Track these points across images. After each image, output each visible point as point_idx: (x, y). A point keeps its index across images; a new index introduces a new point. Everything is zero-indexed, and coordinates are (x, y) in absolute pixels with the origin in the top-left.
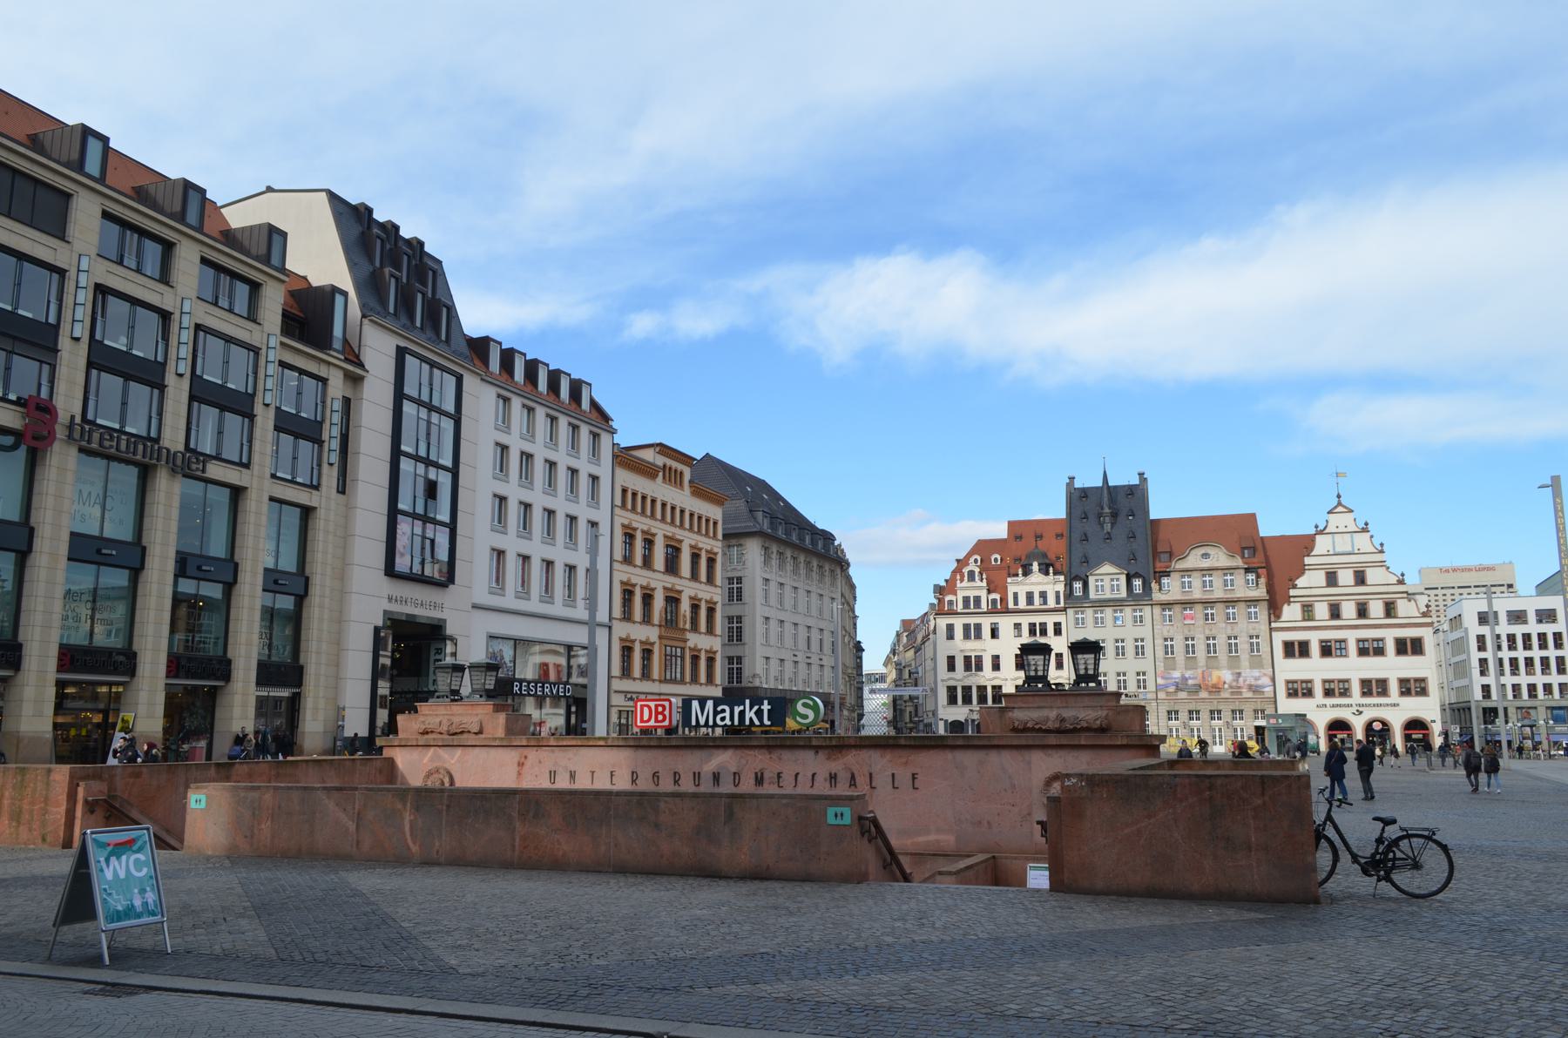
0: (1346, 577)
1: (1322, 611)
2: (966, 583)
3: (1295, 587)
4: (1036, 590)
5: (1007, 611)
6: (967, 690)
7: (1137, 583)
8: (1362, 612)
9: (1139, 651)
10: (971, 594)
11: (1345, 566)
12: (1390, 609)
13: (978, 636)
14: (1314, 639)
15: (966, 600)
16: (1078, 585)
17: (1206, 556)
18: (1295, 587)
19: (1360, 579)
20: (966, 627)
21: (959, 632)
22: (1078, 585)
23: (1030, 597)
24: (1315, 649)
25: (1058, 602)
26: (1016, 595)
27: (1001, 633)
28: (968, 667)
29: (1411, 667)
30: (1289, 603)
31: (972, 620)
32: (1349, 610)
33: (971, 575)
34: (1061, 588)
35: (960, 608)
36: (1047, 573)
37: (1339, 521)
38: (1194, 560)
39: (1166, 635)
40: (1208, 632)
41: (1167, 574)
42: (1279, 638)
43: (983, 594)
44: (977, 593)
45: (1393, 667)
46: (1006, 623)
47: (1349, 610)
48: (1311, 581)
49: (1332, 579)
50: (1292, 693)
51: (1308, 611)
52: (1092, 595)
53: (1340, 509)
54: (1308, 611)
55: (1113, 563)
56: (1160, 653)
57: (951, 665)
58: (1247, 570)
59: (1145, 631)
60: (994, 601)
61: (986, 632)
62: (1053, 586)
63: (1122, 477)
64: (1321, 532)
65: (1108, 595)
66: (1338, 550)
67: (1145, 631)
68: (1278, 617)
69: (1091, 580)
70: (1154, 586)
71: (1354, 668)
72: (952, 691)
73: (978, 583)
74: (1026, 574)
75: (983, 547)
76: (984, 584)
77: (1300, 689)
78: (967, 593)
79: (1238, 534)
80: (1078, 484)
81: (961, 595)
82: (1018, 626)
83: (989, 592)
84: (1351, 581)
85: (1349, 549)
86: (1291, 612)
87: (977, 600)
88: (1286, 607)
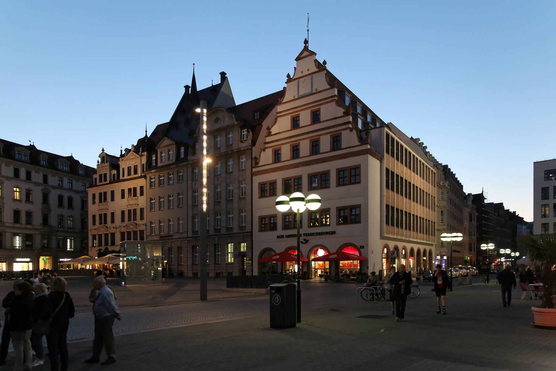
0: (305, 118)
8: (315, 146)
31: (102, 189)
34: (144, 160)
42: (258, 179)
48: (281, 126)
49: (295, 123)
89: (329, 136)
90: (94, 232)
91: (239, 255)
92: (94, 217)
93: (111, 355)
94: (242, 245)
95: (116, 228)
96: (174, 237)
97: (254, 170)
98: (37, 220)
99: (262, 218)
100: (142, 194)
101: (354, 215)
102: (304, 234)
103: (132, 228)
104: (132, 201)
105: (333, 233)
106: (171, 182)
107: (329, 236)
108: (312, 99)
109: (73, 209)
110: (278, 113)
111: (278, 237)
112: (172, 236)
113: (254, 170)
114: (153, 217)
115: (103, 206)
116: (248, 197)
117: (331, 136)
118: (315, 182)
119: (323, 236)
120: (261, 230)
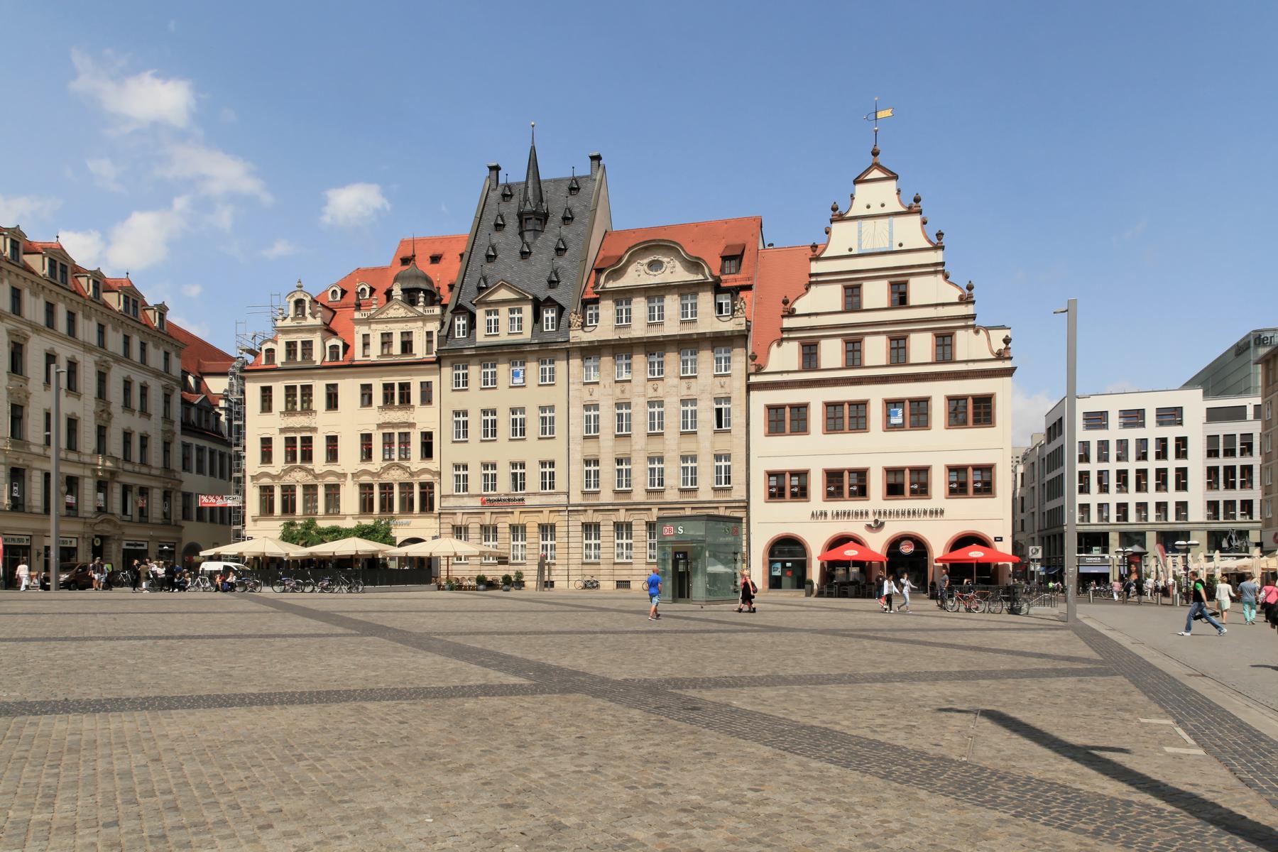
0: (876, 294)
1: (831, 353)
3: (791, 314)
4: (397, 330)
9: (547, 427)
10: (299, 338)
13: (308, 410)
15: (291, 346)
17: (655, 265)
22: (461, 322)
23: (386, 339)
24: (816, 417)
25: (429, 351)
26: (366, 336)
28: (290, 455)
29: (971, 446)
30: (780, 342)
32: (876, 350)
34: (434, 327)
35: (280, 358)
38: (636, 275)
39: (588, 399)
40: (651, 393)
43: (317, 339)
44: (306, 337)
45: (941, 446)
46: (349, 388)
47: (876, 350)
50: (776, 494)
52: (481, 336)
54: (810, 353)
55: (510, 287)
56: (578, 429)
57: (267, 456)
59: (554, 396)
64: (839, 217)
65: (504, 337)
67: (554, 396)
69: (480, 314)
71: (876, 450)
72: (267, 491)
76: (318, 321)
77: (789, 486)
78: (291, 338)
81: (282, 340)
82: (366, 390)
87: (307, 345)
92: (266, 443)
98: (87, 439)
103: (395, 476)
105: (939, 513)
106: (519, 381)
109: (149, 416)
110: (811, 275)
113: (753, 379)
115: (298, 421)
118: (896, 414)
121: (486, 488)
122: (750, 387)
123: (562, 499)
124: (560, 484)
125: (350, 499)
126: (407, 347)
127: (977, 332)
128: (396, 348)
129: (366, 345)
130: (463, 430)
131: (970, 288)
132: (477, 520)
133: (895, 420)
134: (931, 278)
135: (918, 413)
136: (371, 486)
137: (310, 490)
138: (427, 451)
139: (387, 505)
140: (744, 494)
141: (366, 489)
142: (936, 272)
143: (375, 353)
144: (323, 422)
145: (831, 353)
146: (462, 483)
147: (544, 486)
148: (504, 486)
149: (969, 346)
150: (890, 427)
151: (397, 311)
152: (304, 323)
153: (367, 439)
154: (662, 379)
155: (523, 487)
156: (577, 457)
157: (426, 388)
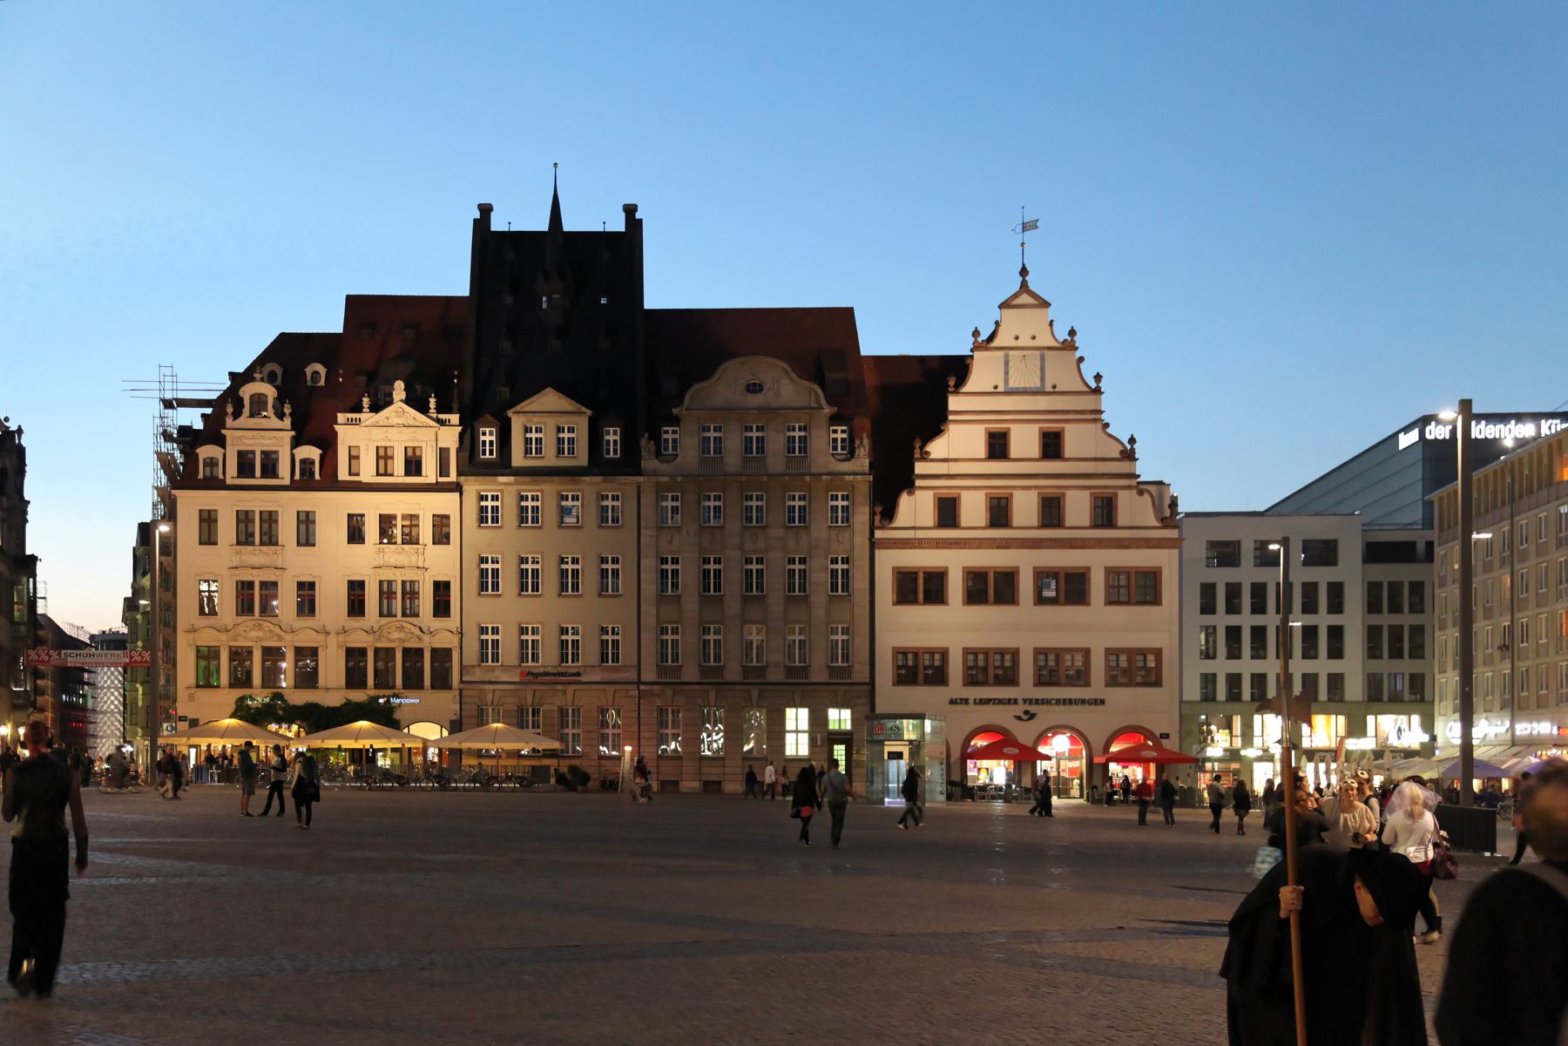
0: (1024, 441)
1: (973, 509)
2: (244, 420)
3: (925, 457)
5: (331, 482)
6: (240, 656)
7: (612, 436)
8: (1052, 511)
11: (1026, 416)
12: (1105, 511)
14: (955, 563)
16: (488, 436)
18: (925, 457)
19: (1052, 446)
20: (244, 518)
21: (227, 529)
22: (488, 436)
23: (383, 456)
24: (955, 587)
25: (443, 469)
27: (322, 530)
31: (257, 502)
32: (1025, 508)
33: (258, 403)
34: (450, 437)
36: (424, 409)
37: (1020, 328)
41: (676, 421)
42: (889, 561)
47: (1025, 508)
48: (956, 446)
49: (998, 446)
51: (948, 511)
52: (518, 459)
53: (1025, 299)
56: (650, 587)
58: (835, 420)
60: (307, 464)
61: (287, 530)
62: (434, 436)
63: (590, 215)
64: (986, 344)
66: (1013, 384)
68: (889, 513)
70: (645, 443)
72: (207, 656)
73: (275, 422)
74: (375, 408)
75: (288, 352)
76: (287, 422)
79: (817, 340)
80: (498, 224)
83: (296, 442)
84: (1035, 451)
85: (1035, 383)
86: (915, 508)
88: (905, 500)
89: (1087, 493)
90: (207, 638)
91: (822, 737)
93: (1236, 819)
94: (846, 714)
95: (328, 633)
96: (584, 679)
97: (879, 534)
99: (901, 653)
100: (441, 537)
101: (1140, 669)
102: (1025, 701)
104: (396, 554)
106: (570, 520)
107: (1086, 707)
108: (1042, 403)
111: (953, 702)
112: (578, 674)
114: (505, 613)
115: (256, 555)
116: (861, 598)
117: (1095, 498)
119: (1074, 708)
120: (1087, 684)
121: (523, 658)
122: (873, 545)
123: (632, 676)
124: (627, 654)
125: (332, 669)
126: (413, 465)
127: (1141, 493)
128: (399, 465)
129: (353, 458)
130: (487, 582)
131: (1132, 440)
132: (513, 700)
133: (1047, 594)
134: (1092, 426)
135: (1073, 588)
136: (363, 651)
137: (272, 654)
138: (442, 607)
139: (383, 680)
140: (867, 674)
141: (355, 656)
142: (1095, 421)
143: (367, 474)
144: (292, 563)
145: (973, 509)
146: (488, 651)
147: (604, 658)
148: (548, 658)
149: (1133, 510)
150: (1040, 600)
151: (399, 411)
152: (264, 423)
153: (356, 589)
154: (763, 528)
155: (575, 658)
156: (649, 621)
157: (441, 522)
